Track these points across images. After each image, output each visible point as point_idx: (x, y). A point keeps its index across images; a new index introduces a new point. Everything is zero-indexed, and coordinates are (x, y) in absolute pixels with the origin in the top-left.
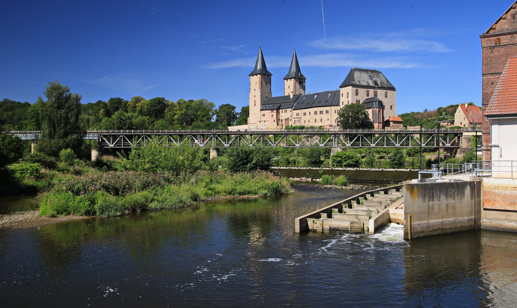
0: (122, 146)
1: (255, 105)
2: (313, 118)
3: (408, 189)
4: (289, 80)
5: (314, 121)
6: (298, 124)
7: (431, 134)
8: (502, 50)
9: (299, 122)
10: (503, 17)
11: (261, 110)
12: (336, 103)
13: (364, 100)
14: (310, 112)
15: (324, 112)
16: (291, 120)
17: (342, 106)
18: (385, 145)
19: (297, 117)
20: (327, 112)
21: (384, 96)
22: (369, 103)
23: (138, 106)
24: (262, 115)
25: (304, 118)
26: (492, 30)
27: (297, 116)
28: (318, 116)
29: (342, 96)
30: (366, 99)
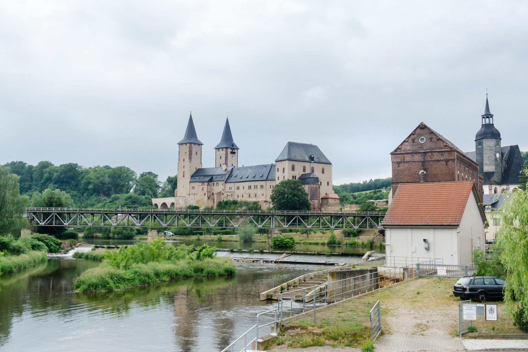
0: (54, 224)
1: (184, 176)
2: (247, 192)
3: (330, 275)
4: (221, 150)
5: (248, 196)
6: (231, 199)
7: (364, 217)
8: (406, 165)
9: (232, 197)
10: (406, 140)
12: (271, 178)
13: (300, 175)
14: (243, 187)
15: (259, 187)
16: (223, 194)
17: (278, 182)
19: (229, 191)
20: (262, 187)
22: (304, 179)
23: (46, 172)
25: (237, 192)
26: (398, 150)
27: (229, 189)
28: (252, 191)
29: (278, 171)
30: (303, 175)
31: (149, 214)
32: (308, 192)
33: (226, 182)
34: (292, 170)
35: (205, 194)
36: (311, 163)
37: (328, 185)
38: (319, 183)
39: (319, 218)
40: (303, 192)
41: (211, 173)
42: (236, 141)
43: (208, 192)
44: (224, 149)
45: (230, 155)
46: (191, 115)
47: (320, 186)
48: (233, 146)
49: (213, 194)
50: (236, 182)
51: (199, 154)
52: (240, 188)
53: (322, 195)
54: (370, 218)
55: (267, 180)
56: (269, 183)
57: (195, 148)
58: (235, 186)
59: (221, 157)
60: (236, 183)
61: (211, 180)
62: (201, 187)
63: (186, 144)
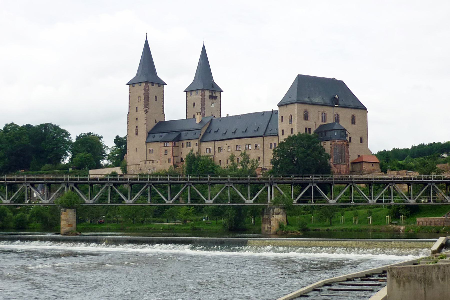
1: (137, 134)
4: (194, 93)
7: (425, 184)
11: (147, 143)
12: (271, 132)
13: (317, 128)
17: (282, 138)
18: (353, 202)
21: (351, 121)
24: (148, 152)
29: (282, 121)
30: (321, 126)
31: (64, 183)
32: (331, 152)
33: (201, 141)
34: (305, 119)
35: (169, 160)
36: (335, 109)
37: (362, 142)
38: (348, 139)
39: (349, 186)
40: (322, 151)
41: (179, 128)
42: (218, 79)
43: (173, 157)
44: (200, 92)
45: (208, 102)
46: (147, 40)
47: (349, 144)
48: (213, 87)
49: (182, 159)
50: (218, 141)
51: (160, 99)
52: (223, 149)
53: (353, 157)
54: (435, 186)
55: (264, 136)
56: (269, 141)
57: (153, 89)
58: (216, 146)
59: (194, 103)
60: (216, 143)
61: (179, 139)
62: (163, 149)
63: (140, 83)
